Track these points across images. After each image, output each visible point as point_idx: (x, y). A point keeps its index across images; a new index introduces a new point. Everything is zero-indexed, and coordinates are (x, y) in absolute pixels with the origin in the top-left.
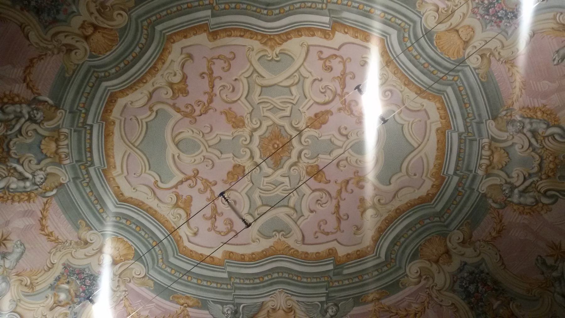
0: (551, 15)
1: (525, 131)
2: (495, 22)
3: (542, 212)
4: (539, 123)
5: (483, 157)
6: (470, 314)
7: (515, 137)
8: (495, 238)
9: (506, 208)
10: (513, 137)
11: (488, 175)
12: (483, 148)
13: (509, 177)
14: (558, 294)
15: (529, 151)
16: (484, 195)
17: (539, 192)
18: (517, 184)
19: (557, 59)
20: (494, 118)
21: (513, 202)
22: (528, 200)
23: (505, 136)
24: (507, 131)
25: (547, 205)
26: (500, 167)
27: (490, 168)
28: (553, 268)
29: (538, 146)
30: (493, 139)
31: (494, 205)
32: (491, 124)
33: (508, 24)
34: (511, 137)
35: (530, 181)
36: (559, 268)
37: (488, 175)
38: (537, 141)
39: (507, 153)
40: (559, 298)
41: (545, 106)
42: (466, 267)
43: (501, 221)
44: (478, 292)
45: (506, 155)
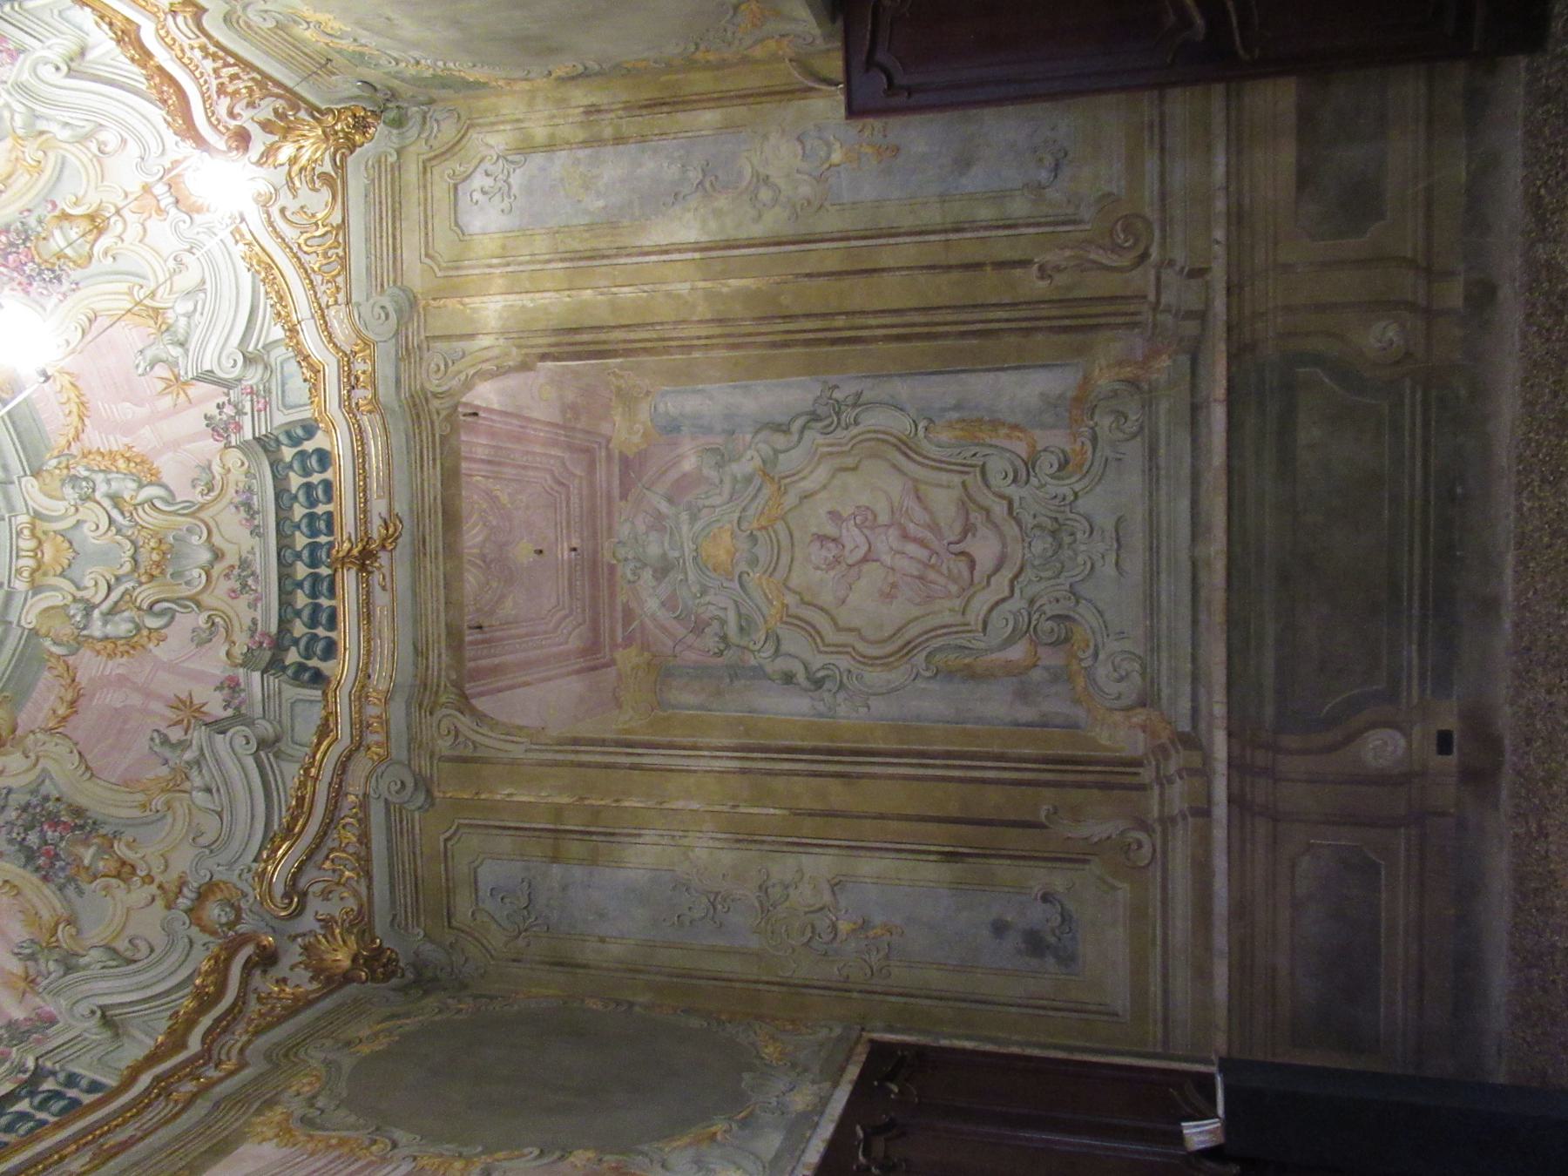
0: (124, 287)
1: (98, 496)
2: (20, 284)
3: (151, 646)
4: (124, 480)
5: (24, 553)
6: (47, 892)
7: (81, 509)
8: (64, 719)
9: (82, 651)
10: (77, 510)
11: (36, 589)
12: (19, 533)
13: (78, 588)
14: (200, 789)
15: (110, 533)
16: (34, 633)
17: (139, 609)
18: (97, 600)
19: (142, 365)
20: (36, 474)
21: (93, 638)
22: (121, 627)
23: (59, 507)
24: (64, 499)
25: (157, 630)
26: (59, 569)
27: (37, 575)
28: (183, 745)
29: (126, 523)
30: (37, 515)
31: (55, 649)
32: (30, 484)
33: (45, 292)
34: (73, 509)
35: (122, 589)
36: (194, 742)
37: (36, 589)
38: (122, 513)
39: (71, 543)
40: (200, 797)
41: (130, 448)
42: (12, 796)
43: (73, 680)
44: (46, 843)
45: (66, 545)
